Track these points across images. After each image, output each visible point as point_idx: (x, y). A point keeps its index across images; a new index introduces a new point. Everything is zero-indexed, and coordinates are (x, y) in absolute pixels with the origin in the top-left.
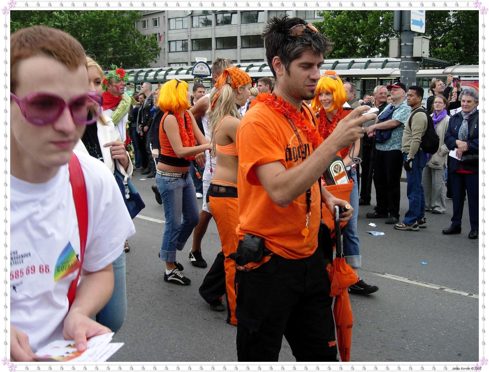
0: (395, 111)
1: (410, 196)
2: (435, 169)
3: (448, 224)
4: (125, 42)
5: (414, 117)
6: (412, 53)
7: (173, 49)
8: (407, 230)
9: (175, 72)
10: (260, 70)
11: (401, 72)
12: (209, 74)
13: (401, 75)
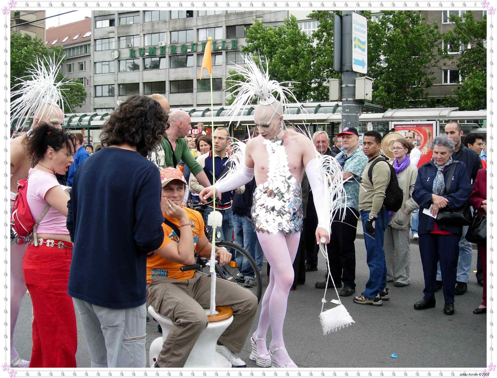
0: (348, 161)
1: (371, 263)
2: (398, 230)
3: (420, 298)
5: (375, 167)
6: (355, 95)
7: (99, 94)
8: (367, 304)
9: (100, 117)
11: (342, 115)
13: (343, 119)
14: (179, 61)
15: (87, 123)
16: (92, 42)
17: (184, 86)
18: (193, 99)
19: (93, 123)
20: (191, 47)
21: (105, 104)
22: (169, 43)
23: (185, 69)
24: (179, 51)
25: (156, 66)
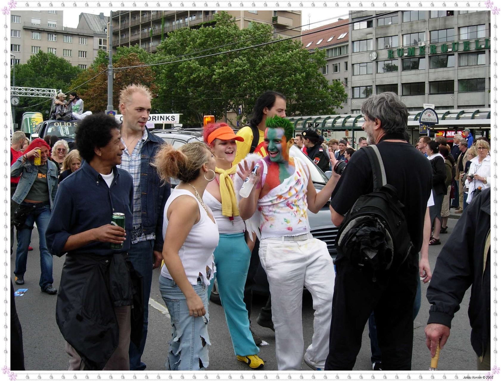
4: (310, 88)
7: (356, 95)
12: (436, 122)
14: (440, 61)
16: (350, 43)
17: (444, 87)
20: (452, 46)
22: (429, 42)
23: (445, 69)
24: (439, 51)
25: (415, 66)
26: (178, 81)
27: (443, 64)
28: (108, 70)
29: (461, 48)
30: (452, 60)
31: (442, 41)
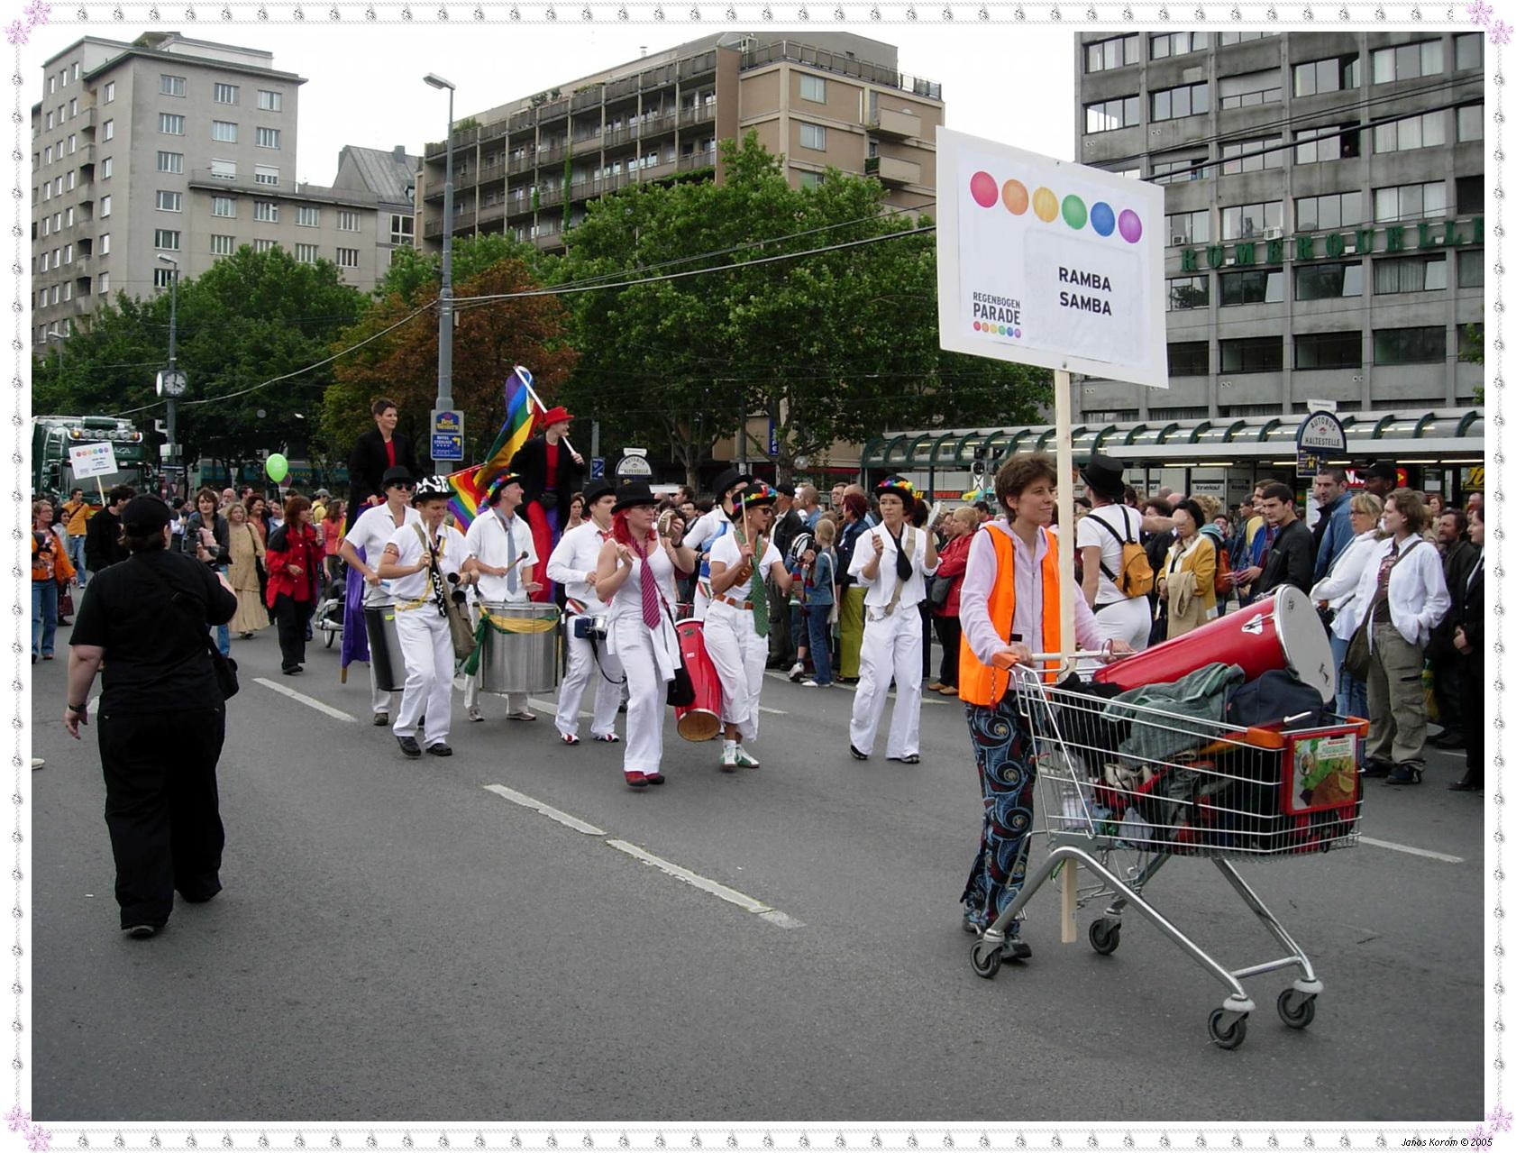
9: (1123, 436)
10: (1377, 435)
14: (1321, 279)
15: (1088, 450)
17: (1334, 350)
18: (1360, 385)
19: (1113, 451)
20: (1355, 240)
21: (1112, 400)
23: (1337, 302)
24: (1320, 252)
25: (1255, 294)
26: (615, 333)
27: (1334, 288)
28: (441, 303)
29: (1381, 246)
30: (1356, 278)
31: (1328, 222)
